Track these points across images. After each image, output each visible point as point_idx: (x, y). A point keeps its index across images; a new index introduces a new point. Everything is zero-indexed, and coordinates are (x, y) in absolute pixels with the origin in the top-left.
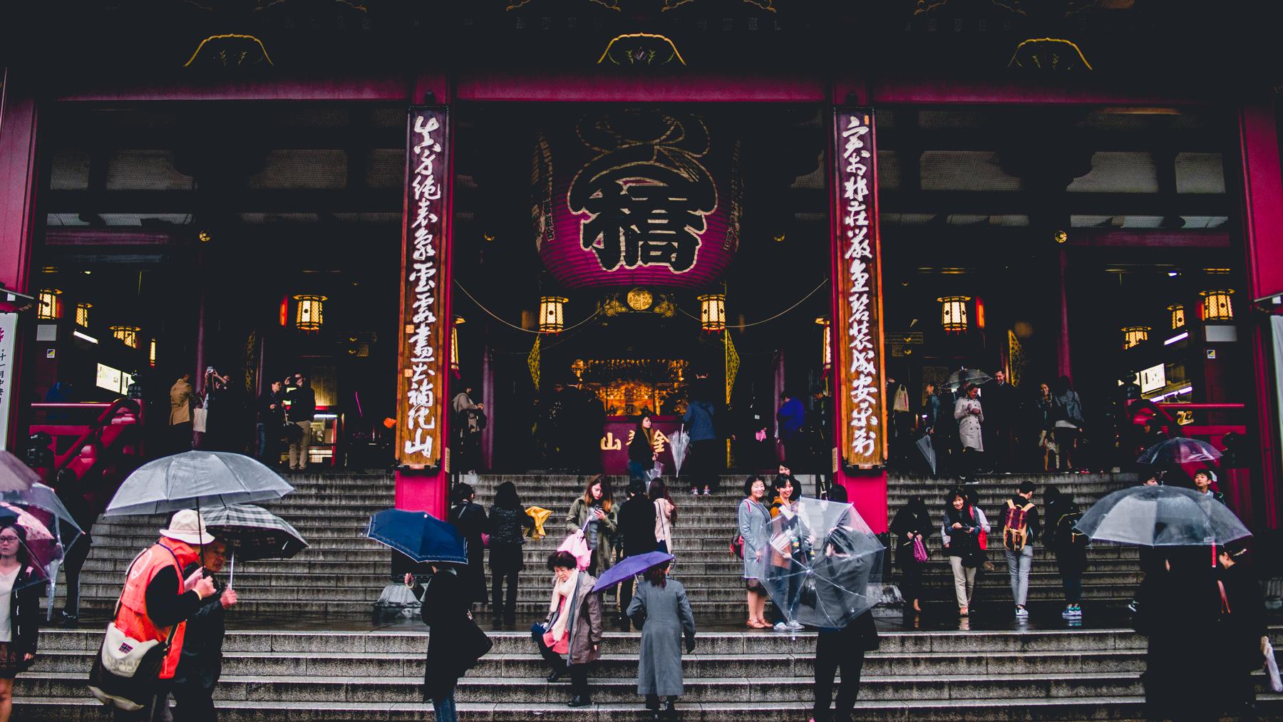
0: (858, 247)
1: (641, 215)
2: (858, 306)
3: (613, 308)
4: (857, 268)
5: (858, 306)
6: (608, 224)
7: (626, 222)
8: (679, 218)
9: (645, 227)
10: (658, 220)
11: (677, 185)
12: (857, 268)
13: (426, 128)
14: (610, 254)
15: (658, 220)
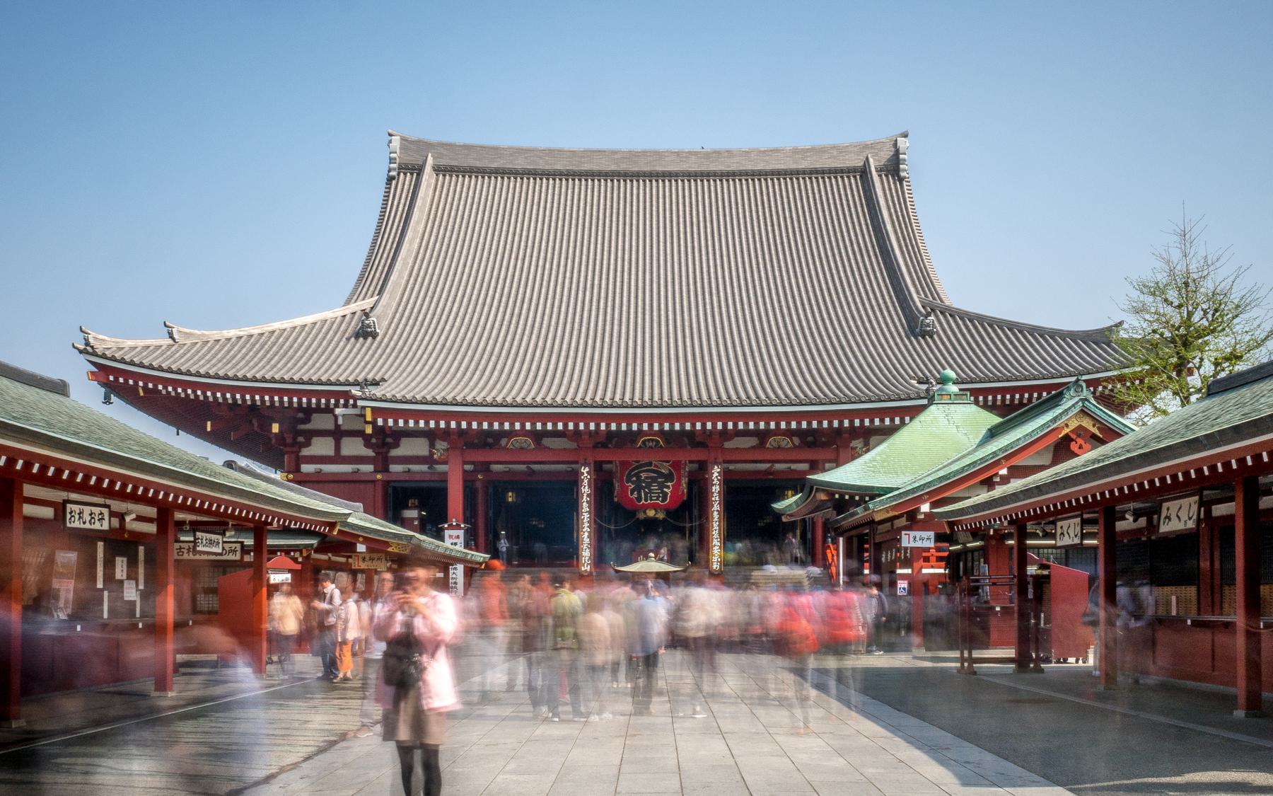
0: (716, 507)
1: (648, 486)
2: (716, 525)
3: (641, 516)
4: (715, 514)
5: (716, 525)
6: (638, 488)
7: (644, 488)
8: (662, 486)
9: (651, 492)
10: (655, 487)
11: (661, 475)
12: (715, 514)
13: (585, 470)
14: (639, 499)
15: (655, 487)
